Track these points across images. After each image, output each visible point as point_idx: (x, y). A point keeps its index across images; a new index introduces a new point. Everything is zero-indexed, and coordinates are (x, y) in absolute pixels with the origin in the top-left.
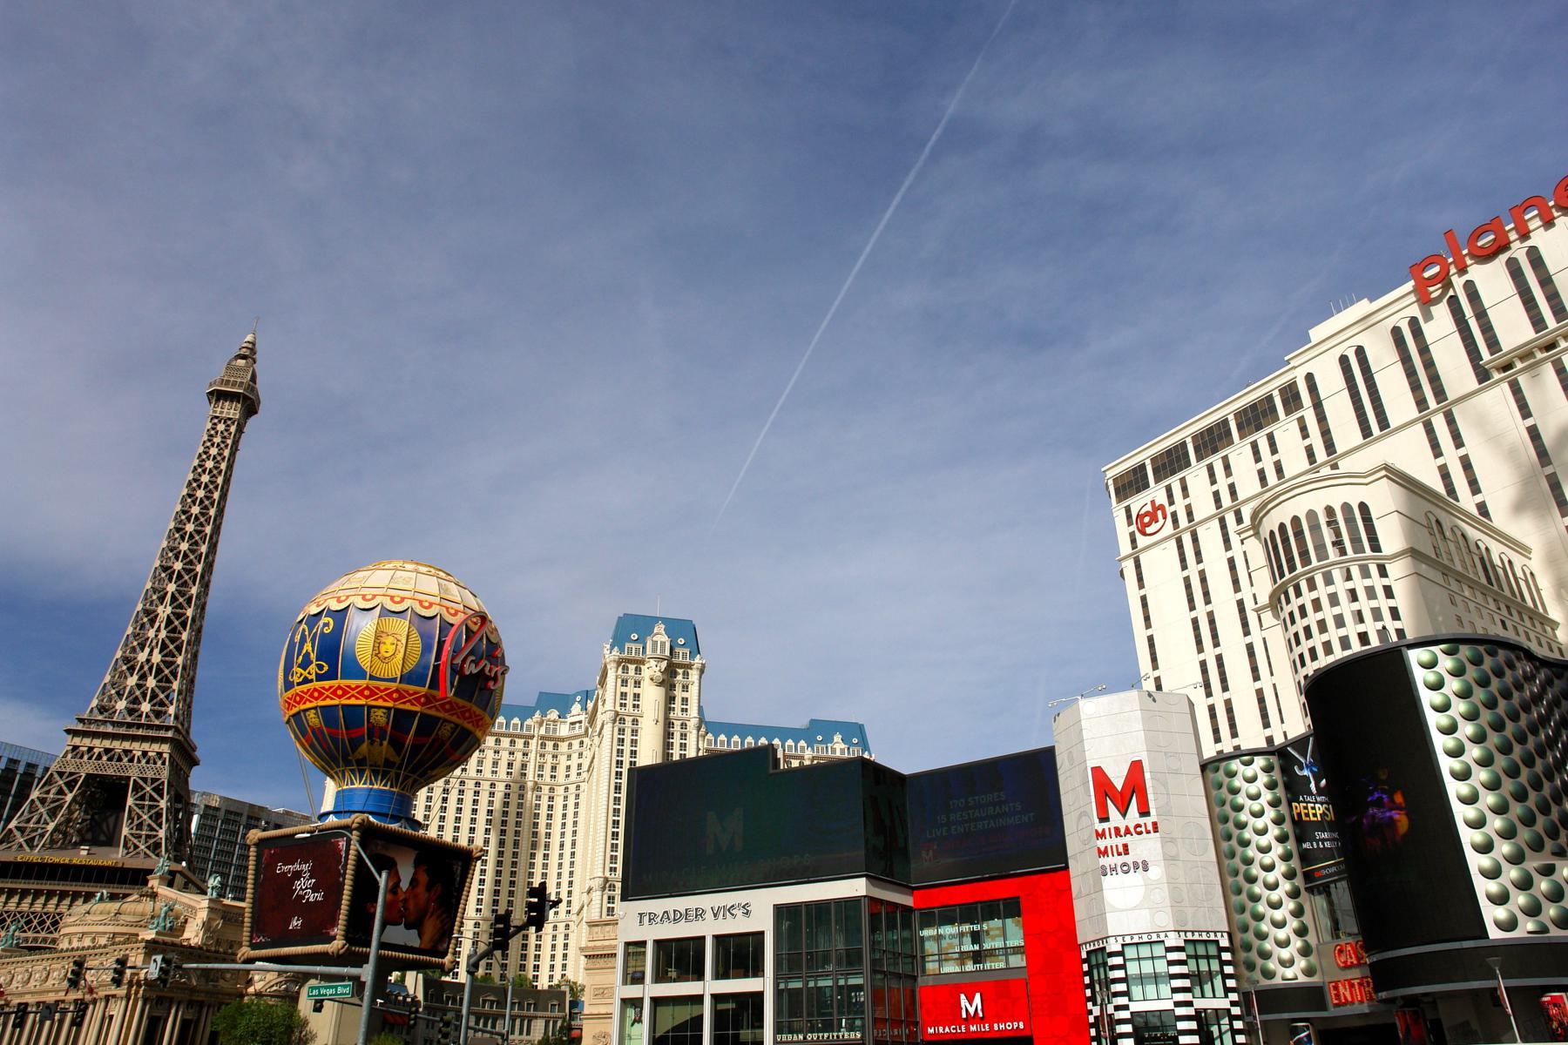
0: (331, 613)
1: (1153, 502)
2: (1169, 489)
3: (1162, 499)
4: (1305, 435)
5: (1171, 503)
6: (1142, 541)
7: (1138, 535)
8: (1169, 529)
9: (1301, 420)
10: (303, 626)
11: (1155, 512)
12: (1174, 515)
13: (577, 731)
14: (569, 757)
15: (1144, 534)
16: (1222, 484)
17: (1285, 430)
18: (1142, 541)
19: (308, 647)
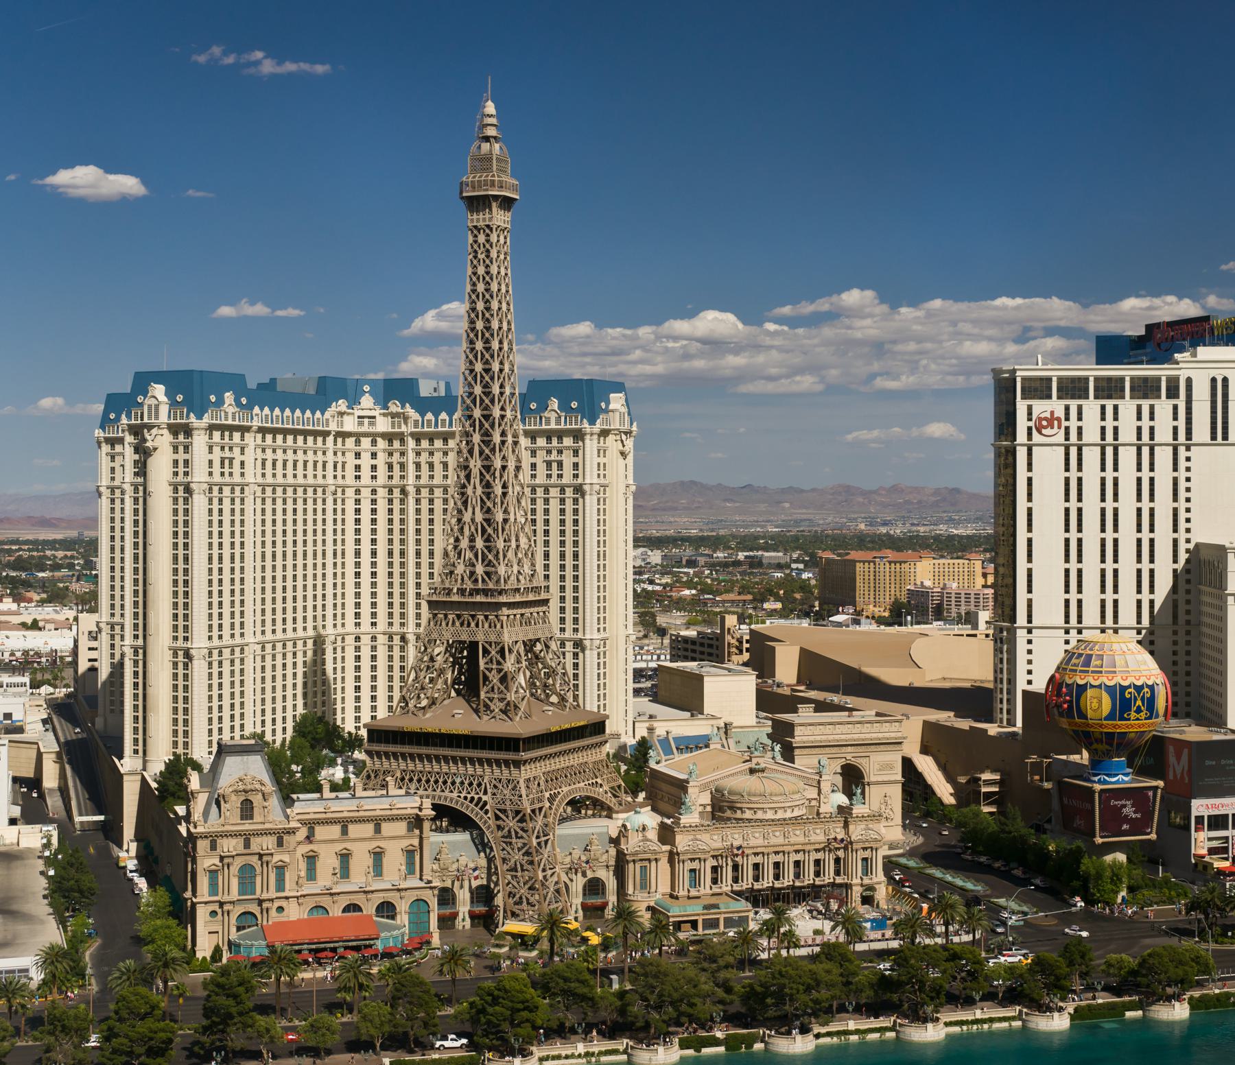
0: (1148, 686)
1: (1052, 413)
2: (1067, 408)
3: (1060, 413)
4: (1175, 418)
5: (1067, 419)
6: (1037, 438)
7: (1034, 431)
8: (1060, 438)
9: (1175, 408)
10: (1132, 690)
11: (1051, 420)
12: (1067, 429)
13: (365, 428)
14: (358, 455)
15: (1040, 433)
16: (1109, 424)
17: (1163, 407)
18: (1037, 438)
19: (1139, 703)
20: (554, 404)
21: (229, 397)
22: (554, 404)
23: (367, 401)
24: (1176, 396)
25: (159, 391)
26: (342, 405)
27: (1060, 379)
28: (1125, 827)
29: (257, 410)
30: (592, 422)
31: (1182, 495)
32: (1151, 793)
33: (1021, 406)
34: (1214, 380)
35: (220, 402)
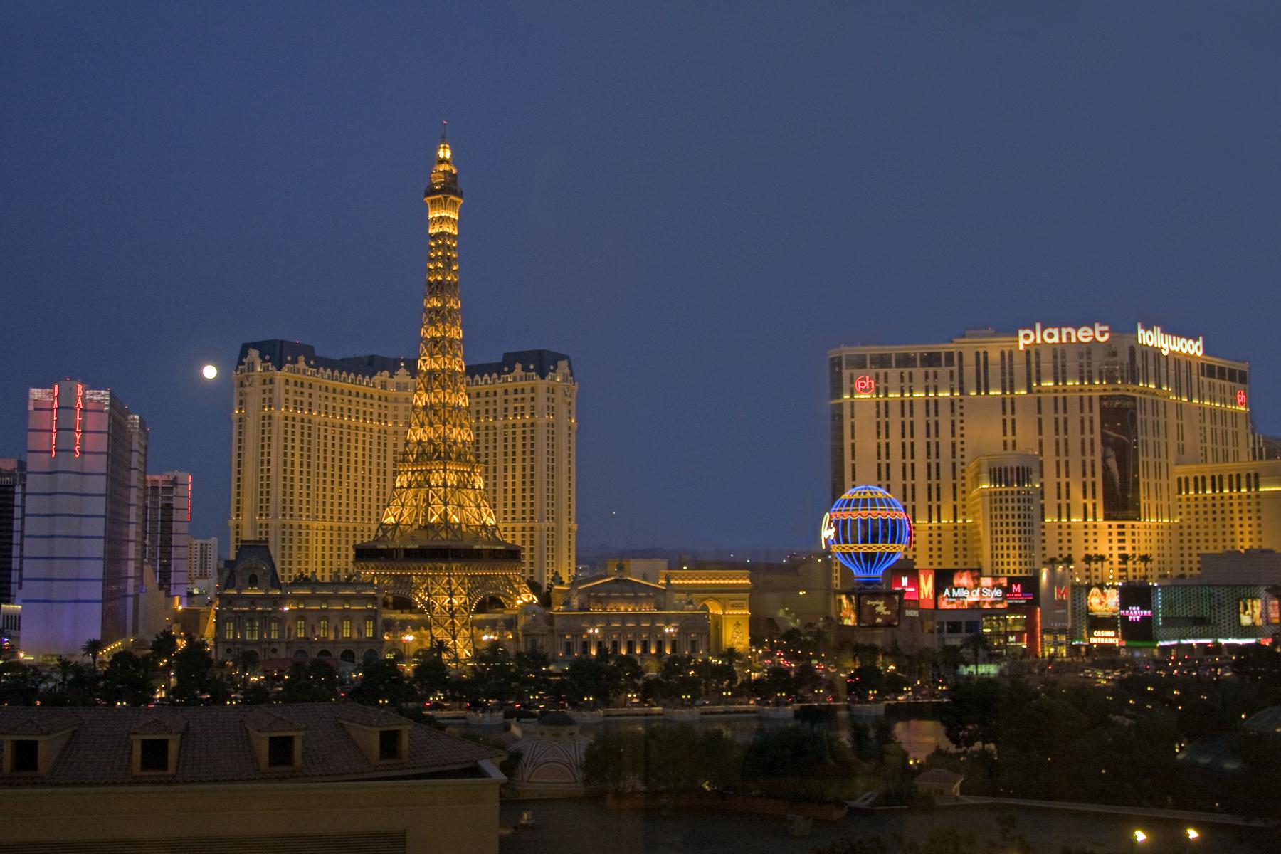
9: (951, 373)
20: (518, 366)
21: (302, 358)
22: (518, 366)
23: (402, 372)
24: (953, 365)
25: (254, 354)
26: (386, 373)
27: (871, 356)
28: (879, 620)
29: (321, 370)
30: (543, 378)
31: (958, 432)
32: (897, 597)
33: (846, 374)
34: (977, 354)
35: (295, 361)
